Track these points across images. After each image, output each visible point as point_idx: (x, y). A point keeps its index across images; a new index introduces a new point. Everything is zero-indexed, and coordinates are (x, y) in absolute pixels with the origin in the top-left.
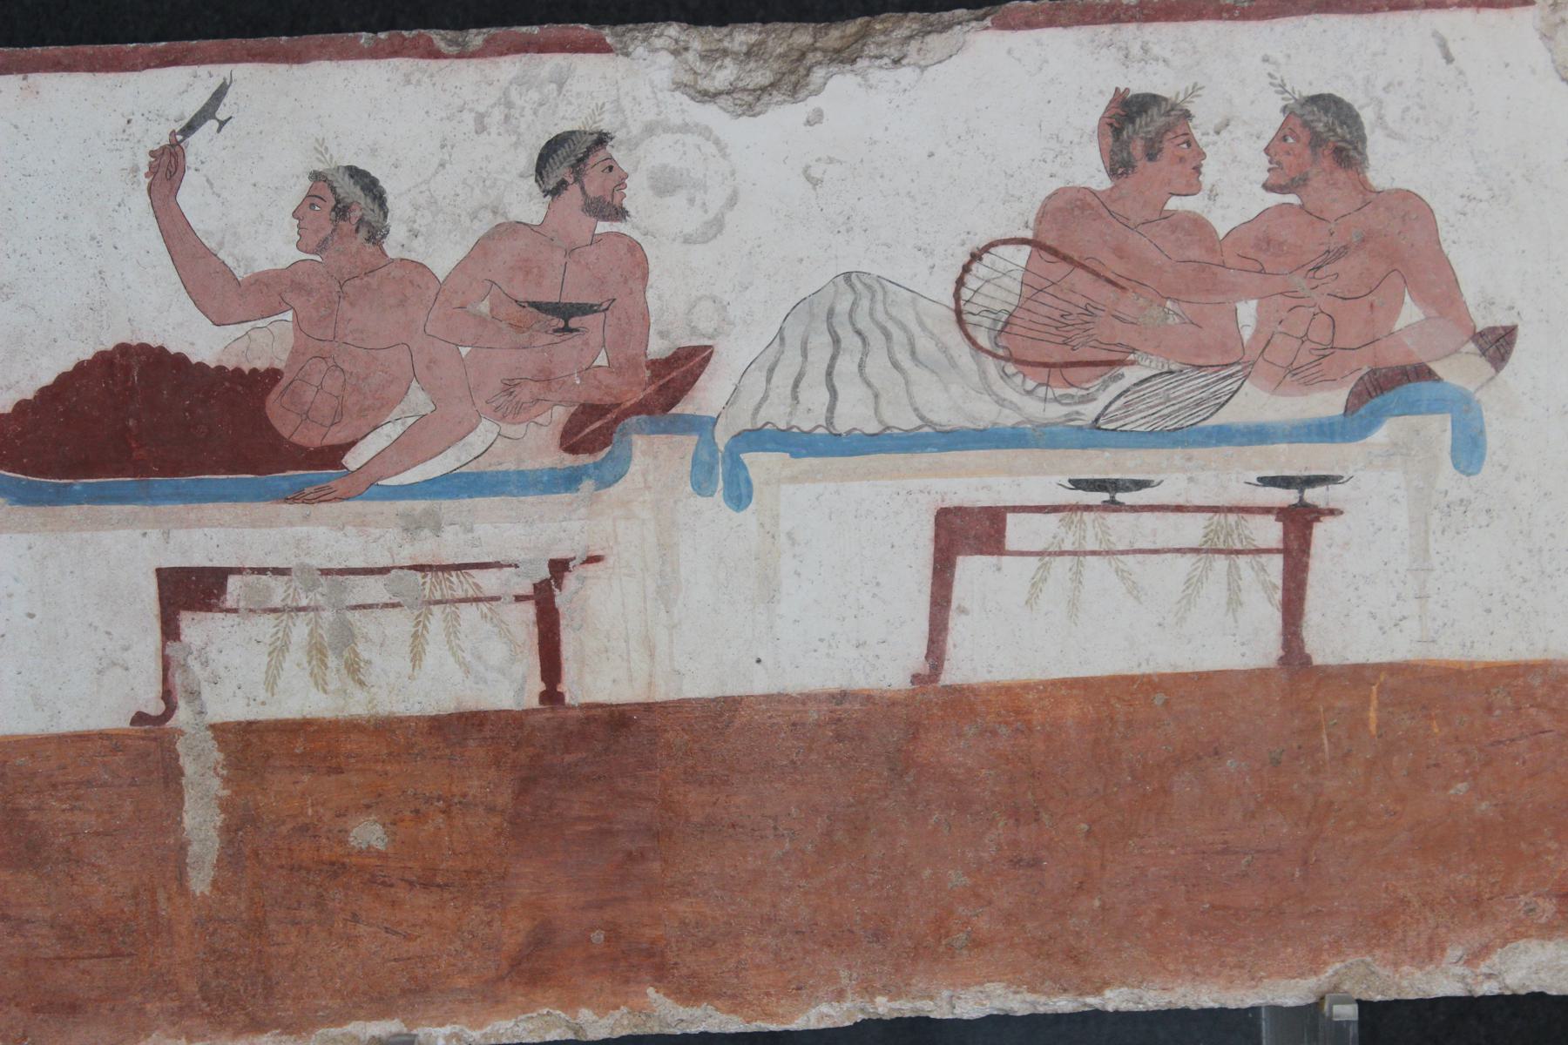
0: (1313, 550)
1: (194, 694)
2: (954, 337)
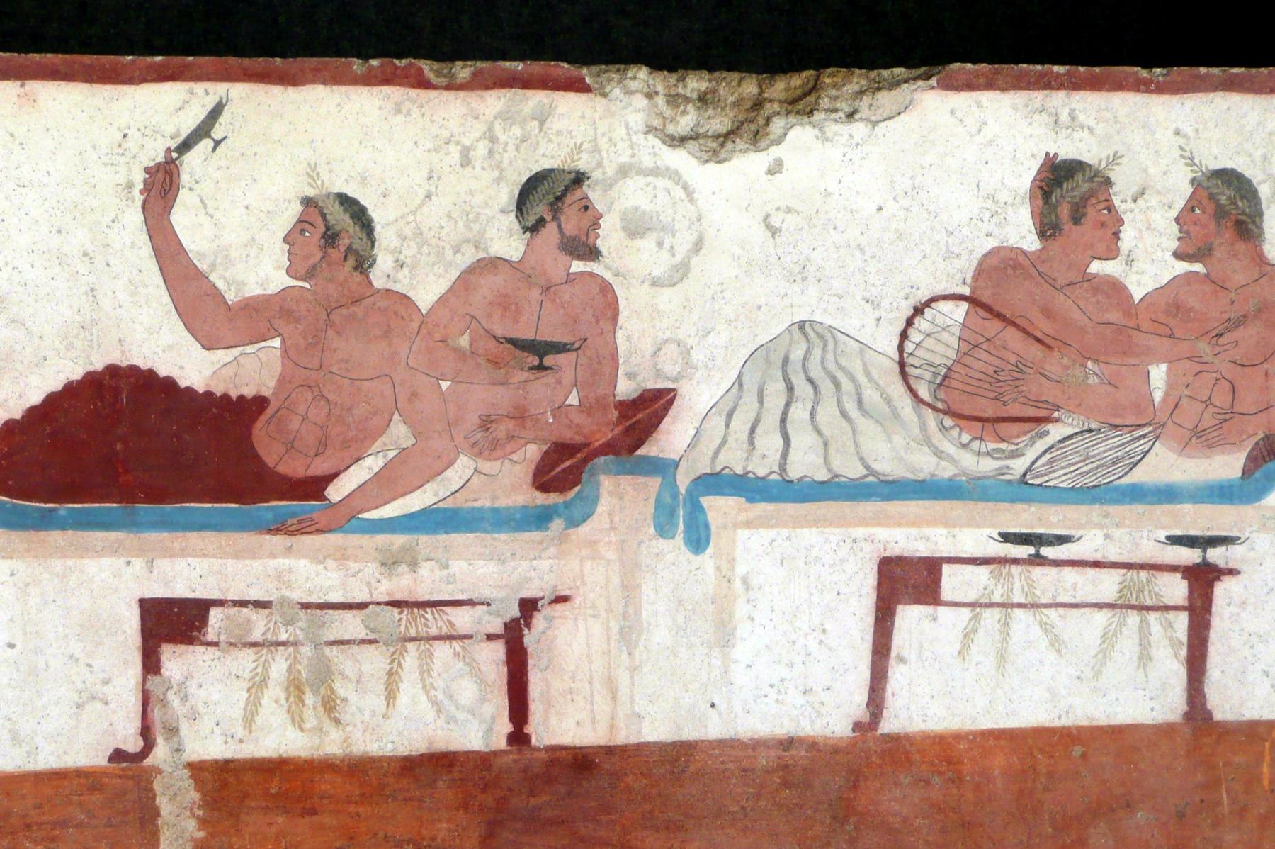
0: (1214, 609)
1: (172, 731)
2: (897, 389)
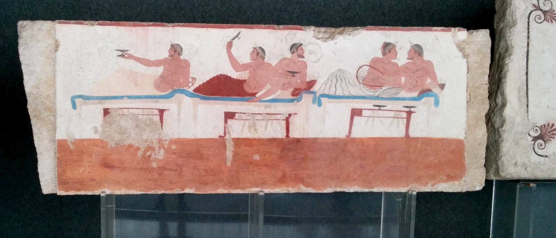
1: (229, 133)
2: (356, 80)
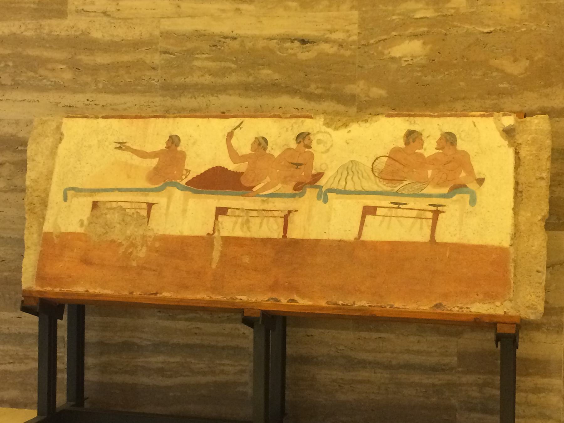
1: (219, 230)
2: (371, 173)
